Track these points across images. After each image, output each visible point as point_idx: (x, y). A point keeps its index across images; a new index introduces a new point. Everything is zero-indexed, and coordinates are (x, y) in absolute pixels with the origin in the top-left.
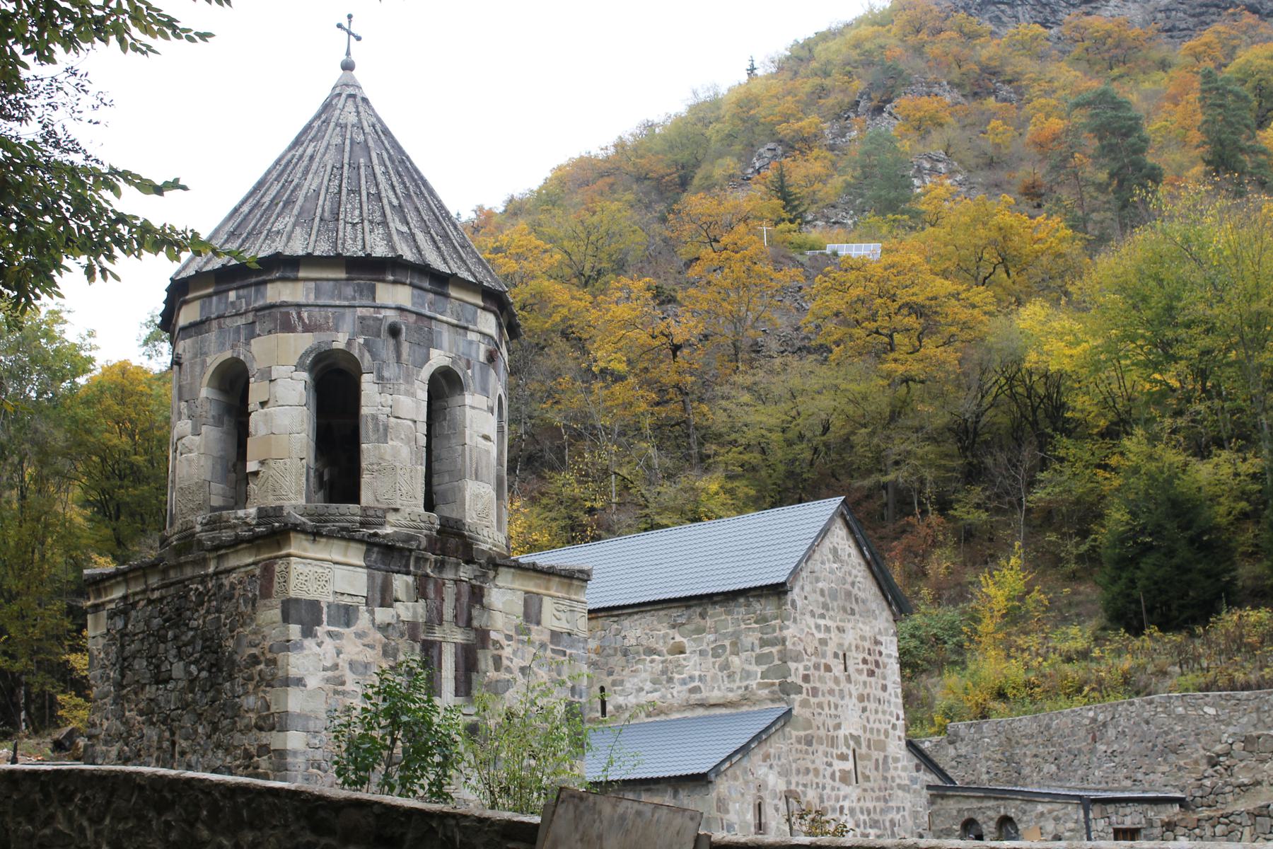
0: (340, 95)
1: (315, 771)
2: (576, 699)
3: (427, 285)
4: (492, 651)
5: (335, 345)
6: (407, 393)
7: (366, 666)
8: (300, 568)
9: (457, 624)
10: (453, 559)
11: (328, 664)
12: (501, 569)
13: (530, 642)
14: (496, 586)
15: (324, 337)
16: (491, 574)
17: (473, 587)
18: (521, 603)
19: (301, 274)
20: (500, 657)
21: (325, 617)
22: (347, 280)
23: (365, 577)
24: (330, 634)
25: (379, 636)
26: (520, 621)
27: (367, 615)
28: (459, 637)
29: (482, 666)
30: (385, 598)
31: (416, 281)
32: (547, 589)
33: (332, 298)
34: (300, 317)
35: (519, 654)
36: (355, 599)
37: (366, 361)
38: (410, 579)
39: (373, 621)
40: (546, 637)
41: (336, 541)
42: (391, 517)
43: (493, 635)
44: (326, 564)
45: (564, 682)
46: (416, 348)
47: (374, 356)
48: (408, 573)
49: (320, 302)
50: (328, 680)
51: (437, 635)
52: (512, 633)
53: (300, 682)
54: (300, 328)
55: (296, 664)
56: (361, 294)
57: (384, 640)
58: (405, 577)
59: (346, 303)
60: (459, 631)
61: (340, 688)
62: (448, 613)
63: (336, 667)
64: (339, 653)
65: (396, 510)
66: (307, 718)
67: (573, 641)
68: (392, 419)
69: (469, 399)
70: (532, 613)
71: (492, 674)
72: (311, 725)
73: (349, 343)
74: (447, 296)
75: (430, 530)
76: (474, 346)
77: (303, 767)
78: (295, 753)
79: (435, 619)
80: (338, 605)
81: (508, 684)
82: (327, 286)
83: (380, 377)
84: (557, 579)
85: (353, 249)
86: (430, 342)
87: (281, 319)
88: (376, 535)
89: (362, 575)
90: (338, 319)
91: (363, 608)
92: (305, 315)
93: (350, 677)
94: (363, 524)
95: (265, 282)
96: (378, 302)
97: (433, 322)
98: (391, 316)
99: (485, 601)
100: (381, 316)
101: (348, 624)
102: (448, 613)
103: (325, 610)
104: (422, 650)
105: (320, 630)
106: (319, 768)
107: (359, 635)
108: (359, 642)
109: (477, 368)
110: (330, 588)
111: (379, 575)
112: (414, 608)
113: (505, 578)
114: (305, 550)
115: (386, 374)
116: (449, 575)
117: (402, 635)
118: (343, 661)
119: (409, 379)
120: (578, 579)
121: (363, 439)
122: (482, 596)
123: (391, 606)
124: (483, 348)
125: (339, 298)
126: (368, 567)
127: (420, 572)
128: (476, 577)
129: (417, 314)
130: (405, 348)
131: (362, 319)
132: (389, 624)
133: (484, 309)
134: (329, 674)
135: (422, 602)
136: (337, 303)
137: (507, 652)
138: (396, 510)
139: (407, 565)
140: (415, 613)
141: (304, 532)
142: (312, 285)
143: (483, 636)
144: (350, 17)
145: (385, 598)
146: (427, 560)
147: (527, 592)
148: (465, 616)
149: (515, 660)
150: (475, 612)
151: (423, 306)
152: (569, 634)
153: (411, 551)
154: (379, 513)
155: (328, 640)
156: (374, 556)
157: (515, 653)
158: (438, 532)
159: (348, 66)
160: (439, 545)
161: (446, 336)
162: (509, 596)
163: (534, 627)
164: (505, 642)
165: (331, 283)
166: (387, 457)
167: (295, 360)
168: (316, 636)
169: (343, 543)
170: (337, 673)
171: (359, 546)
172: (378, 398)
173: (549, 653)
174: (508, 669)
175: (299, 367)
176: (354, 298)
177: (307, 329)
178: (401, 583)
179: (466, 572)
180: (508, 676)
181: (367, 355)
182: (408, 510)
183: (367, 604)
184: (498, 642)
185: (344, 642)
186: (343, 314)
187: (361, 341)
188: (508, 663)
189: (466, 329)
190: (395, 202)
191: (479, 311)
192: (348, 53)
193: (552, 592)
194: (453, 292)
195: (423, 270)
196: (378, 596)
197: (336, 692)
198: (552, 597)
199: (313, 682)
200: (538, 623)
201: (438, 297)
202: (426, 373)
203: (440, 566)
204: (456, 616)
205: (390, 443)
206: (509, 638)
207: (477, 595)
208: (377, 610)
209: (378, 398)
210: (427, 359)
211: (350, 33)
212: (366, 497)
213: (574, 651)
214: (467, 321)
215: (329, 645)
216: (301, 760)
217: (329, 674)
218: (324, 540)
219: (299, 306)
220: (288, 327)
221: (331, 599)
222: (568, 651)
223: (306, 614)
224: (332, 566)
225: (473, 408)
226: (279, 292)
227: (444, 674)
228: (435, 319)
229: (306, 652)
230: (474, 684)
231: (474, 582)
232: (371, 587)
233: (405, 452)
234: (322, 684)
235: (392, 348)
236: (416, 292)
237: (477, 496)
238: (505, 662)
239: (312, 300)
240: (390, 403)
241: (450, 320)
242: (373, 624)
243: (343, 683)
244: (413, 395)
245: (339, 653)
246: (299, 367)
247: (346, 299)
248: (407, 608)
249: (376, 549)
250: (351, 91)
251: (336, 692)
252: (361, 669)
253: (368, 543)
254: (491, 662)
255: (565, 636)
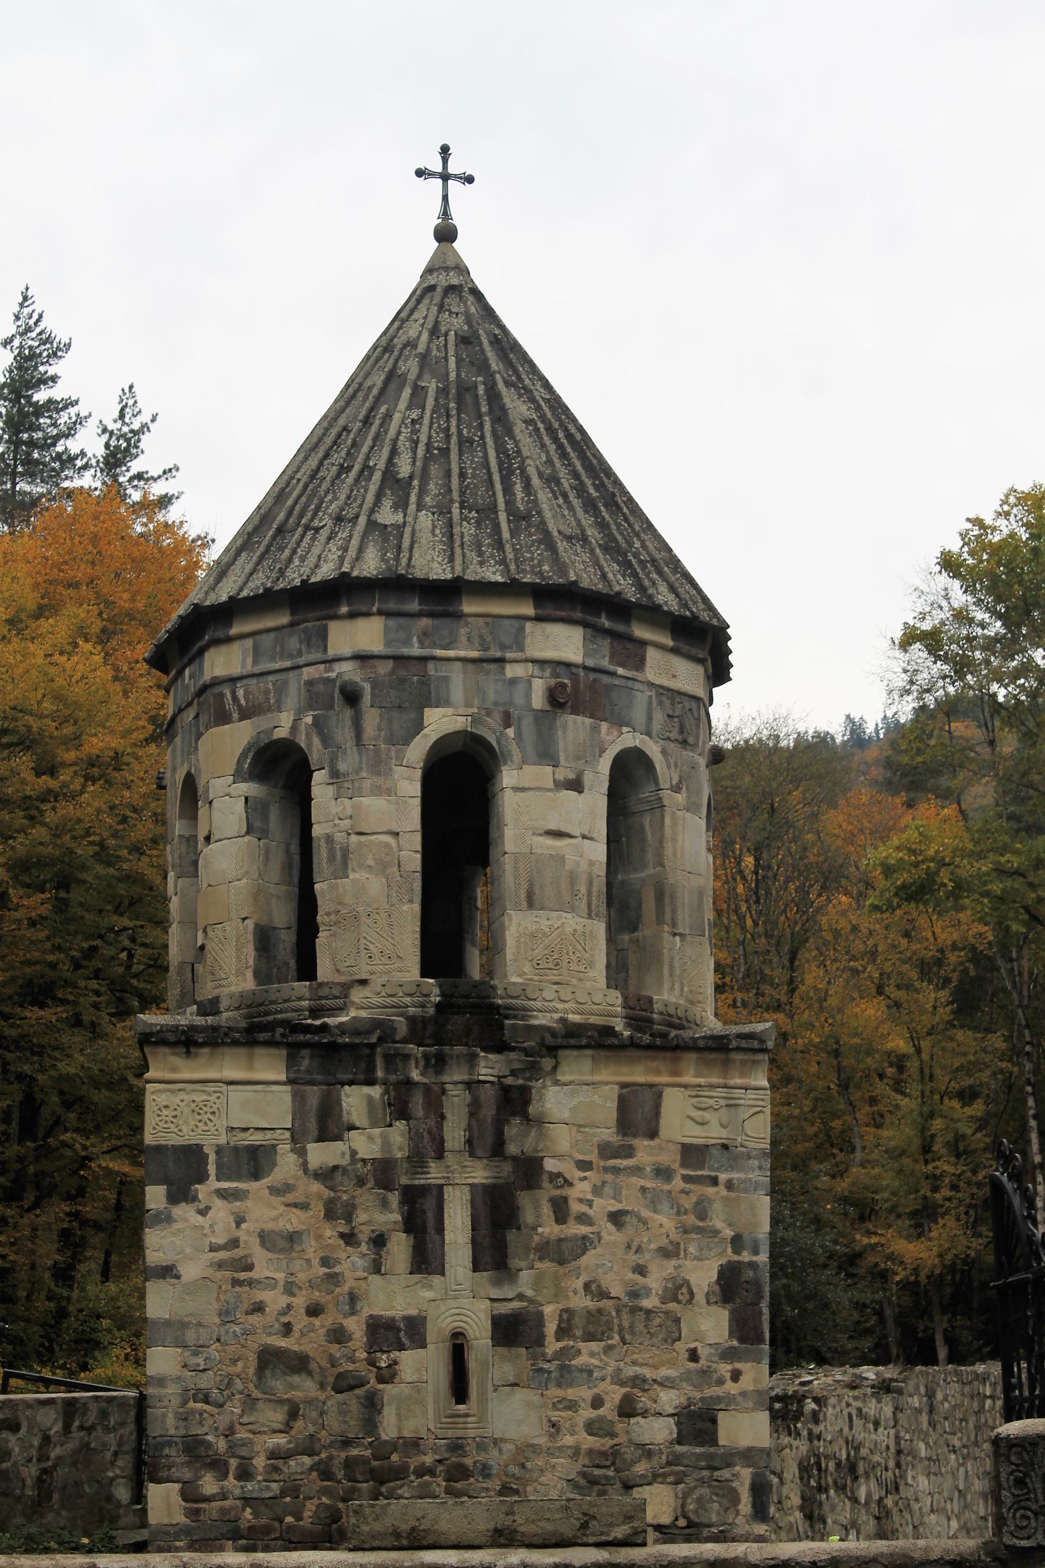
0: (432, 288)
1: (199, 1405)
2: (746, 1256)
3: (414, 606)
4: (548, 1191)
5: (282, 733)
6: (377, 791)
7: (293, 1238)
8: (163, 1099)
9: (472, 1154)
10: (458, 1049)
11: (221, 1241)
12: (561, 1053)
13: (637, 1170)
14: (557, 1083)
15: (262, 722)
16: (547, 1063)
17: (505, 1091)
18: (612, 1105)
19: (234, 631)
20: (565, 1199)
21: (212, 1169)
22: (292, 625)
23: (288, 1098)
24: (221, 1194)
25: (316, 1187)
26: (608, 1134)
27: (292, 1157)
28: (480, 1174)
29: (528, 1216)
30: (329, 1125)
31: (392, 606)
32: (675, 1073)
33: (273, 659)
34: (235, 698)
35: (607, 1190)
36: (269, 1135)
37: (316, 751)
38: (376, 1092)
39: (305, 1165)
40: (670, 1158)
41: (227, 1050)
42: (357, 995)
43: (550, 1165)
44: (210, 1088)
45: (716, 1232)
46: (395, 714)
47: (326, 741)
48: (370, 1082)
49: (257, 669)
50: (220, 1265)
51: (434, 1174)
52: (593, 1157)
53: (168, 1272)
54: (235, 716)
55: (158, 1245)
56: (309, 646)
57: (327, 1193)
58: (366, 1090)
59: (288, 664)
60: (480, 1164)
61: (243, 1276)
62: (454, 1133)
63: (234, 1243)
64: (239, 1221)
65: (363, 982)
66: (184, 1325)
67: (736, 1158)
68: (354, 838)
69: (508, 777)
70: (637, 1116)
71: (549, 1229)
72: (190, 1336)
73: (294, 728)
74: (459, 616)
75: (423, 1006)
76: (521, 687)
77: (176, 1401)
78: (161, 1381)
79: (430, 1147)
80: (236, 1149)
81: (584, 1244)
82: (267, 640)
83: (335, 774)
84: (693, 1055)
85: (294, 577)
86: (428, 696)
87: (214, 704)
88: (324, 1027)
89: (284, 1096)
90: (281, 689)
91: (284, 1148)
92: (240, 693)
93: (260, 1256)
94: (314, 1013)
95: (201, 652)
96: (331, 652)
97: (431, 666)
98: (347, 670)
99: (531, 1110)
100: (333, 675)
101: (256, 1176)
102: (454, 1133)
103: (212, 1158)
104: (402, 1203)
105: (202, 1190)
106: (206, 1401)
107: (275, 1191)
108: (276, 1201)
109: (528, 723)
110: (222, 1123)
111: (314, 1094)
112: (385, 1138)
113: (576, 1068)
114: (174, 1069)
115: (342, 767)
116: (455, 1075)
117: (361, 1182)
118: (247, 1234)
119: (379, 767)
120: (738, 1049)
121: (316, 877)
122: (527, 1102)
123: (338, 1138)
124: (539, 689)
125: (282, 657)
126: (290, 1081)
127: (393, 1078)
128: (513, 1073)
129: (394, 658)
130: (372, 719)
131: (310, 683)
132: (336, 1168)
133: (538, 619)
134: (223, 1255)
135: (400, 1125)
136: (278, 665)
137: (581, 1189)
138: (363, 982)
139: (371, 1069)
140: (386, 1144)
141: (163, 1042)
142: (249, 643)
143: (529, 1171)
144: (445, 150)
145: (329, 1125)
146: (407, 1057)
147: (624, 1086)
148: (489, 1139)
149: (598, 1202)
150: (513, 1129)
151: (407, 642)
152: (725, 1147)
153: (372, 1047)
154: (336, 991)
155: (218, 1203)
156: (305, 1063)
157: (597, 1190)
158: (439, 1007)
159: (446, 234)
160: (430, 1030)
161: (458, 681)
162: (584, 1095)
163: (641, 1144)
164: (574, 1173)
165: (273, 635)
166: (348, 900)
167: (231, 768)
168: (195, 1199)
169: (242, 1051)
170: (237, 1253)
171: (274, 1051)
172: (335, 808)
173: (678, 1183)
174: (583, 1219)
175: (239, 776)
176: (300, 654)
177: (245, 715)
178: (355, 1100)
179: (489, 1067)
180: (584, 1230)
181: (316, 741)
182: (384, 979)
183: (294, 1140)
184: (559, 1175)
185: (249, 1203)
186: (286, 683)
187: (309, 720)
188: (584, 1208)
189: (501, 661)
190: (404, 469)
191: (529, 626)
192: (445, 213)
193: (687, 1079)
194: (469, 607)
195: (395, 586)
196: (312, 1125)
197: (236, 1282)
198: (685, 1086)
199: (190, 1271)
200: (653, 1134)
201: (438, 622)
202: (418, 751)
203: (437, 1063)
204: (469, 1142)
205: (352, 876)
206: (584, 1166)
207: (514, 1101)
208: (311, 1147)
209: (335, 808)
210: (418, 726)
211: (445, 177)
212: (324, 970)
213: (735, 1175)
214: (503, 647)
215: (221, 1212)
216: (172, 1390)
217: (223, 1255)
218: (205, 1050)
219: (233, 680)
220: (223, 718)
221: (223, 1140)
222: (723, 1177)
223: (184, 1170)
224: (225, 1087)
225: (517, 789)
226: (221, 662)
227: (448, 1237)
228: (434, 658)
229: (177, 1226)
230: (511, 1250)
231: (510, 1081)
232: (299, 1112)
233: (375, 885)
234: (209, 1272)
235: (348, 723)
236: (392, 622)
237: (533, 936)
238: (575, 1207)
239: (249, 668)
240: (349, 811)
241: (462, 653)
242: (306, 1171)
243: (250, 1268)
244: (389, 792)
245: (239, 1221)
246: (239, 776)
247: (291, 656)
248: (371, 1138)
249: (305, 1052)
250: (442, 280)
251: (236, 1282)
252: (282, 1243)
253: (289, 1045)
254: (546, 1210)
255: (715, 1152)
